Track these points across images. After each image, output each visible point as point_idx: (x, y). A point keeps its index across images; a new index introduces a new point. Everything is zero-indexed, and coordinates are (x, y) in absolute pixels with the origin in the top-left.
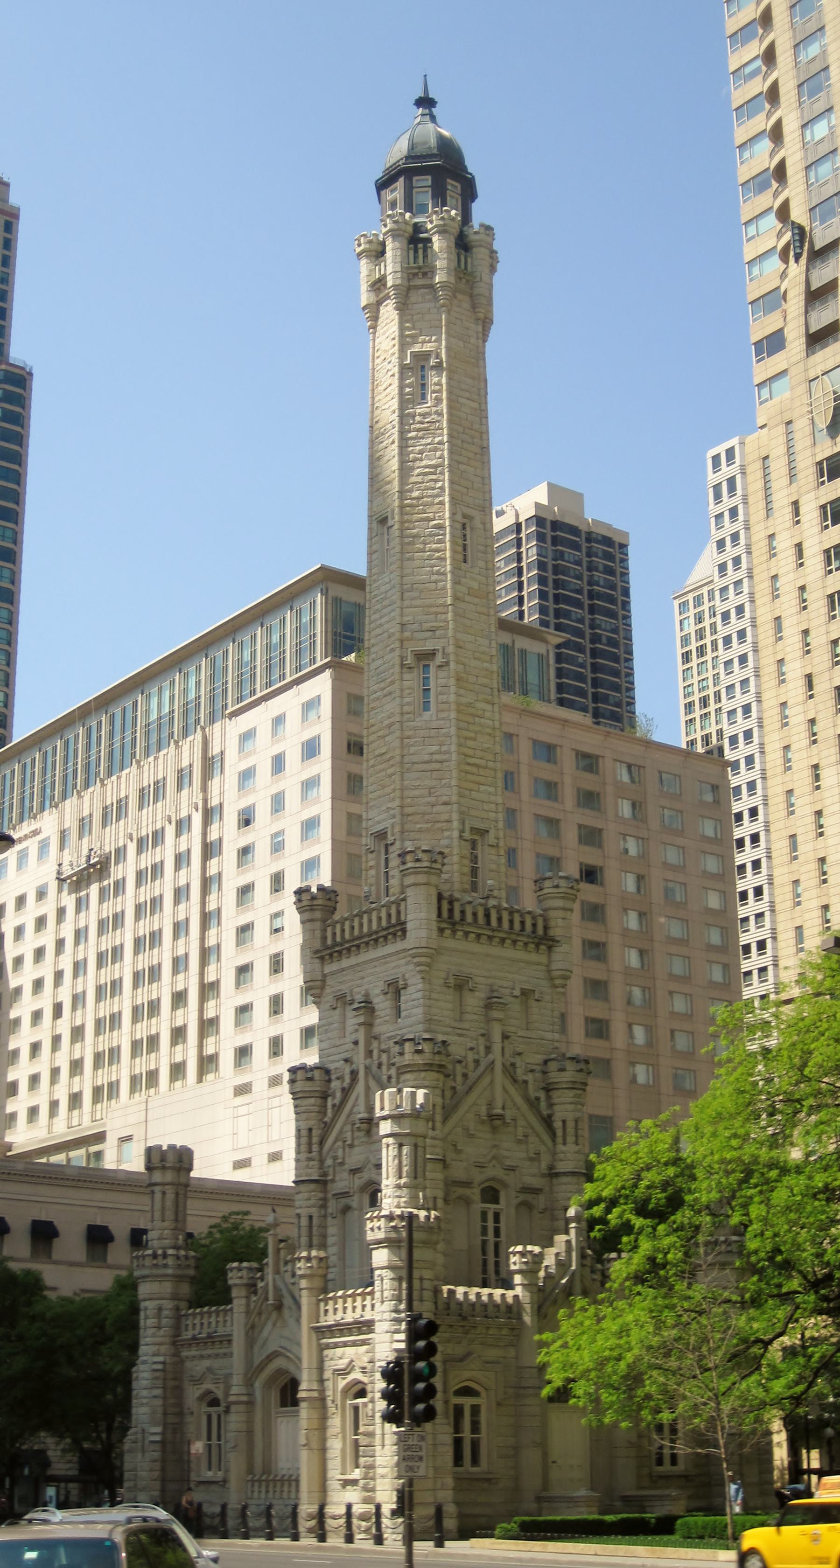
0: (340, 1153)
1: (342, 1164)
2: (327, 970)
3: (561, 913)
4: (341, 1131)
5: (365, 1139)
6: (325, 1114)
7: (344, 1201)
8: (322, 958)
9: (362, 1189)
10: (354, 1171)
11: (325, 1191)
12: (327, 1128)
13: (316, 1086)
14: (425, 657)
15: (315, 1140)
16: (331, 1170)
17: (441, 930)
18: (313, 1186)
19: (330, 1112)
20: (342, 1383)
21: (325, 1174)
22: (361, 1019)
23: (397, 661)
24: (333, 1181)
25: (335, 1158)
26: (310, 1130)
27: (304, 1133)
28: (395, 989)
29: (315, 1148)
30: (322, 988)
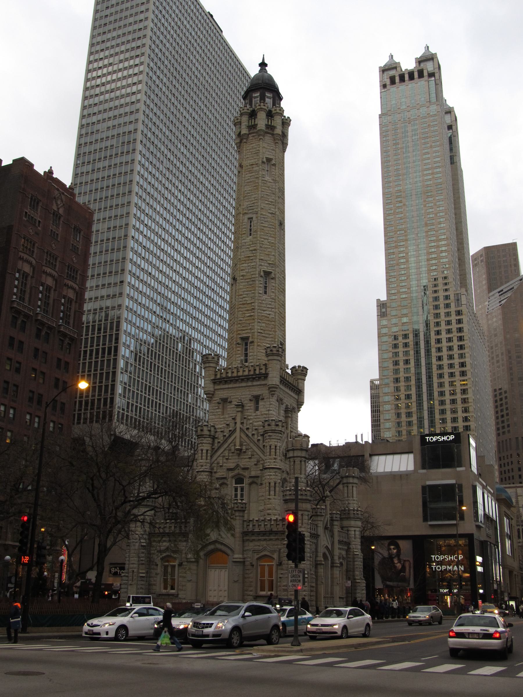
0: (221, 462)
1: (221, 466)
2: (217, 387)
4: (222, 453)
5: (237, 457)
6: (213, 444)
7: (221, 481)
8: (214, 383)
9: (232, 477)
10: (229, 470)
11: (211, 476)
12: (214, 451)
13: (212, 433)
14: (267, 274)
15: (209, 455)
16: (215, 468)
18: (207, 473)
19: (216, 445)
20: (256, 556)
21: (212, 469)
22: (240, 409)
23: (257, 272)
24: (215, 472)
25: (218, 463)
26: (207, 451)
27: (204, 451)
28: (257, 399)
29: (209, 458)
30: (213, 395)
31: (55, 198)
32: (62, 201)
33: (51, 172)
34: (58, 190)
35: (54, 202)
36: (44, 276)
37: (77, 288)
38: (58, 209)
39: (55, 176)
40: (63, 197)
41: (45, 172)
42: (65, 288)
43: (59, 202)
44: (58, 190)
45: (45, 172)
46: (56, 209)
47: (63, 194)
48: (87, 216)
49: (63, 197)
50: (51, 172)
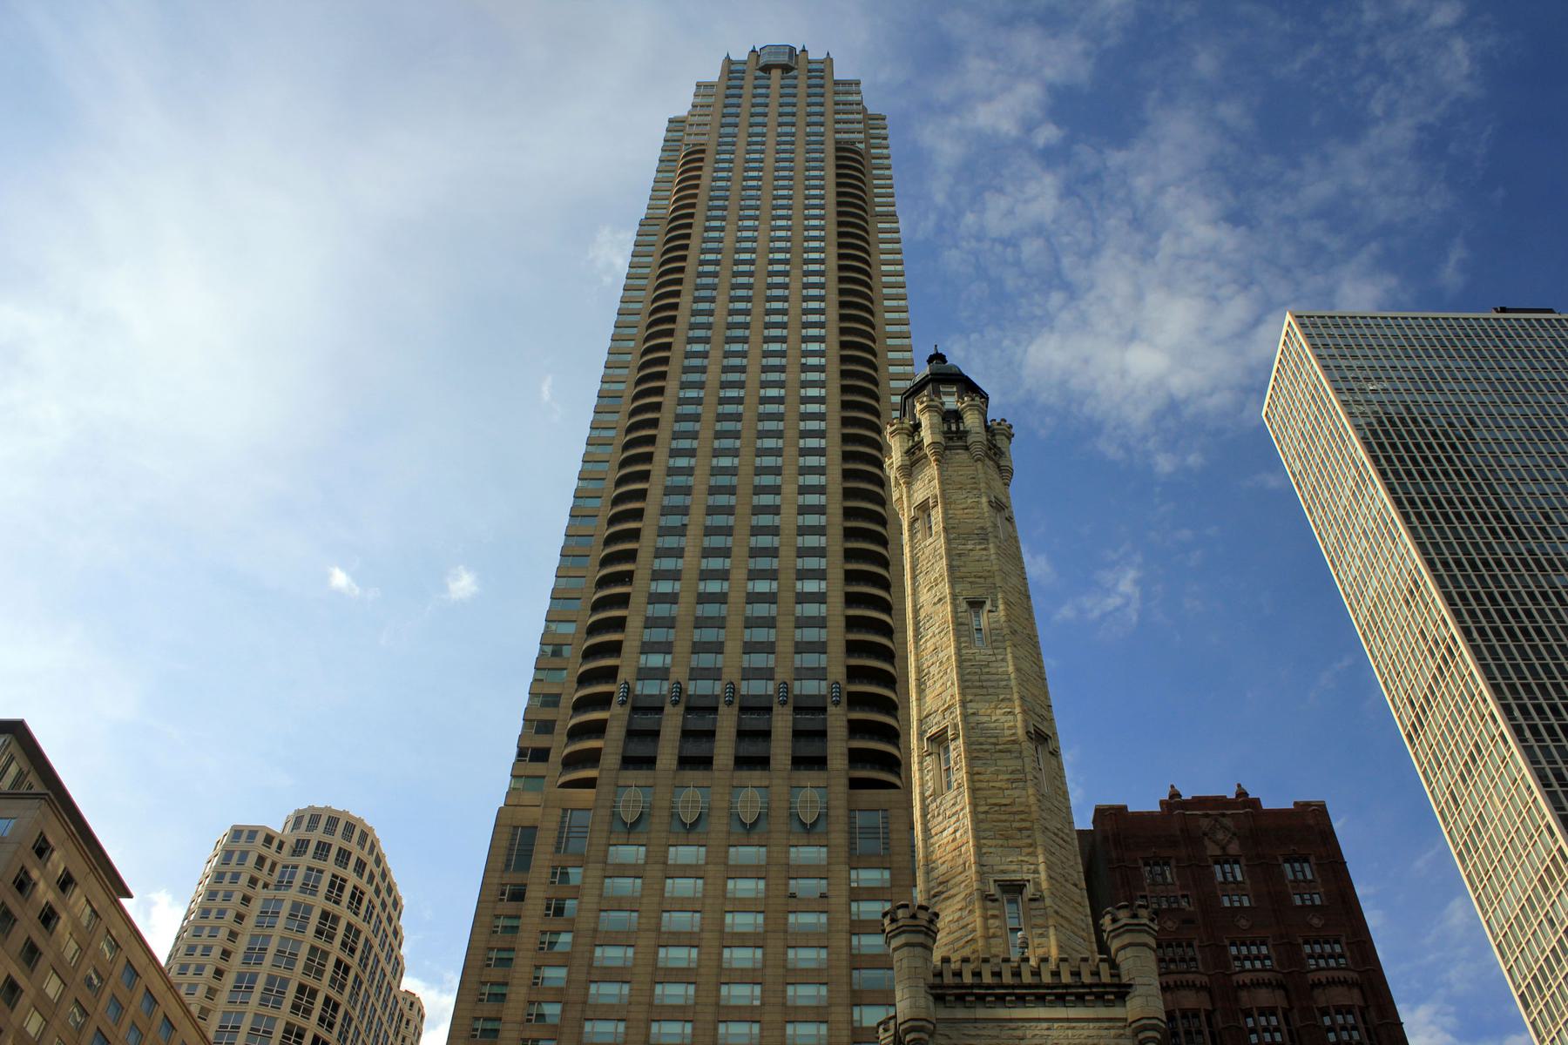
3: (1129, 952)
17: (939, 999)
31: (1205, 834)
32: (1226, 829)
33: (1175, 795)
34: (1207, 816)
35: (1206, 841)
36: (1244, 994)
37: (1356, 976)
38: (1223, 848)
39: (1186, 796)
40: (1224, 821)
41: (1162, 803)
42: (1316, 992)
43: (1220, 836)
44: (1207, 816)
45: (1162, 803)
46: (1218, 852)
47: (1224, 815)
48: (1311, 822)
49: (1226, 821)
50: (1175, 795)
